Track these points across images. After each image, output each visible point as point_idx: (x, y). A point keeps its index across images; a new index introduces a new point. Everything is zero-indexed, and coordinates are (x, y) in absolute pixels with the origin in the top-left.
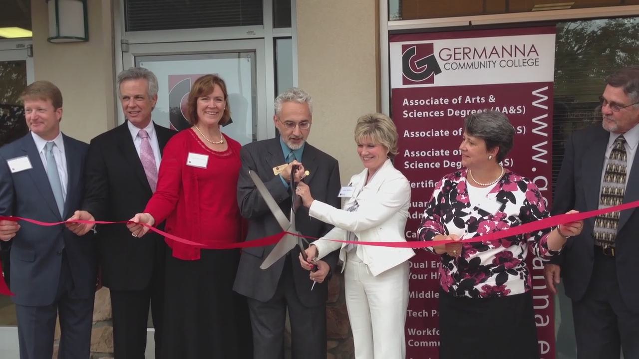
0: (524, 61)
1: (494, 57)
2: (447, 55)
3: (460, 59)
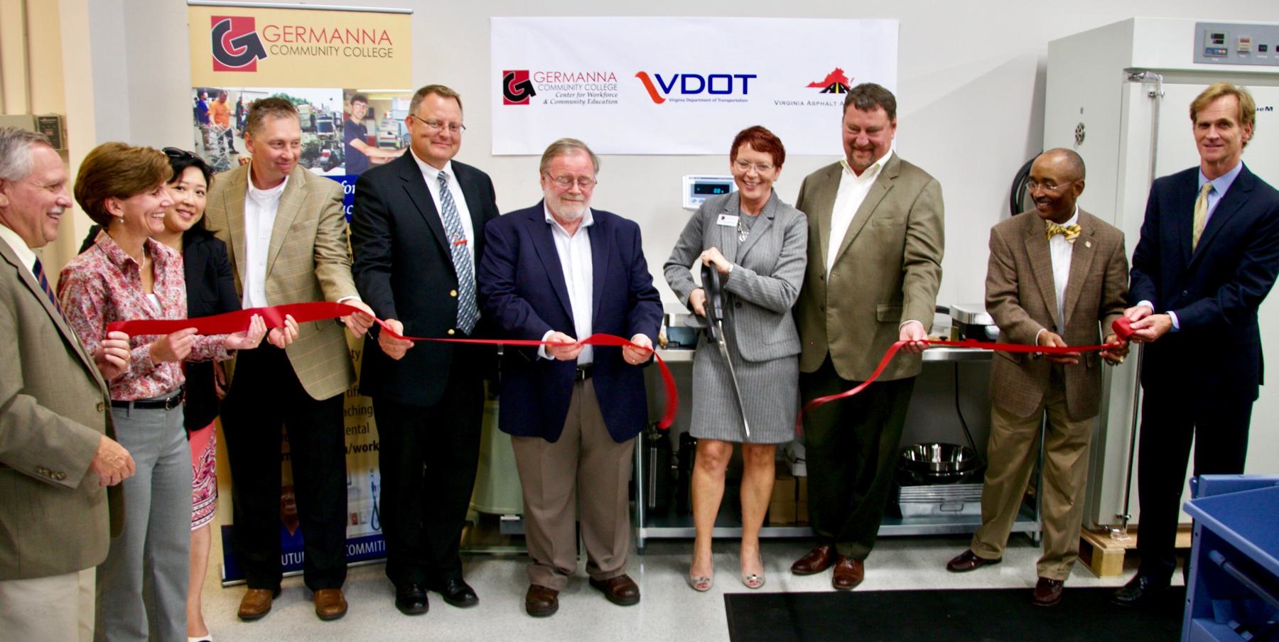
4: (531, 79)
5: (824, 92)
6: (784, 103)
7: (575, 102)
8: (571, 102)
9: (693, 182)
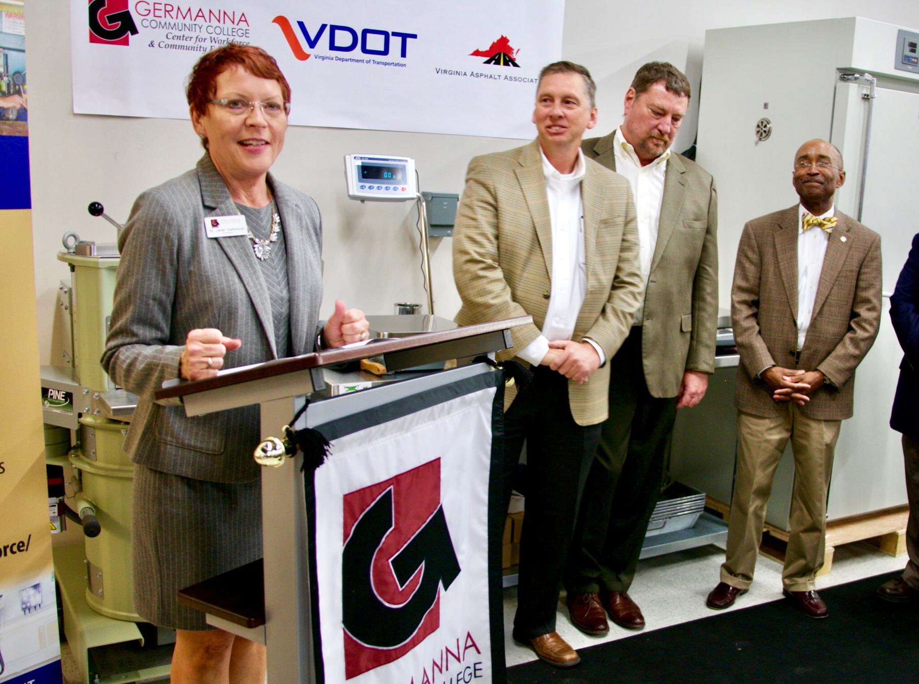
0: (234, 30)
1: (200, 21)
2: (146, 10)
3: (161, 17)
5: (488, 62)
6: (445, 72)
7: (193, 48)
8: (188, 48)
9: (359, 163)
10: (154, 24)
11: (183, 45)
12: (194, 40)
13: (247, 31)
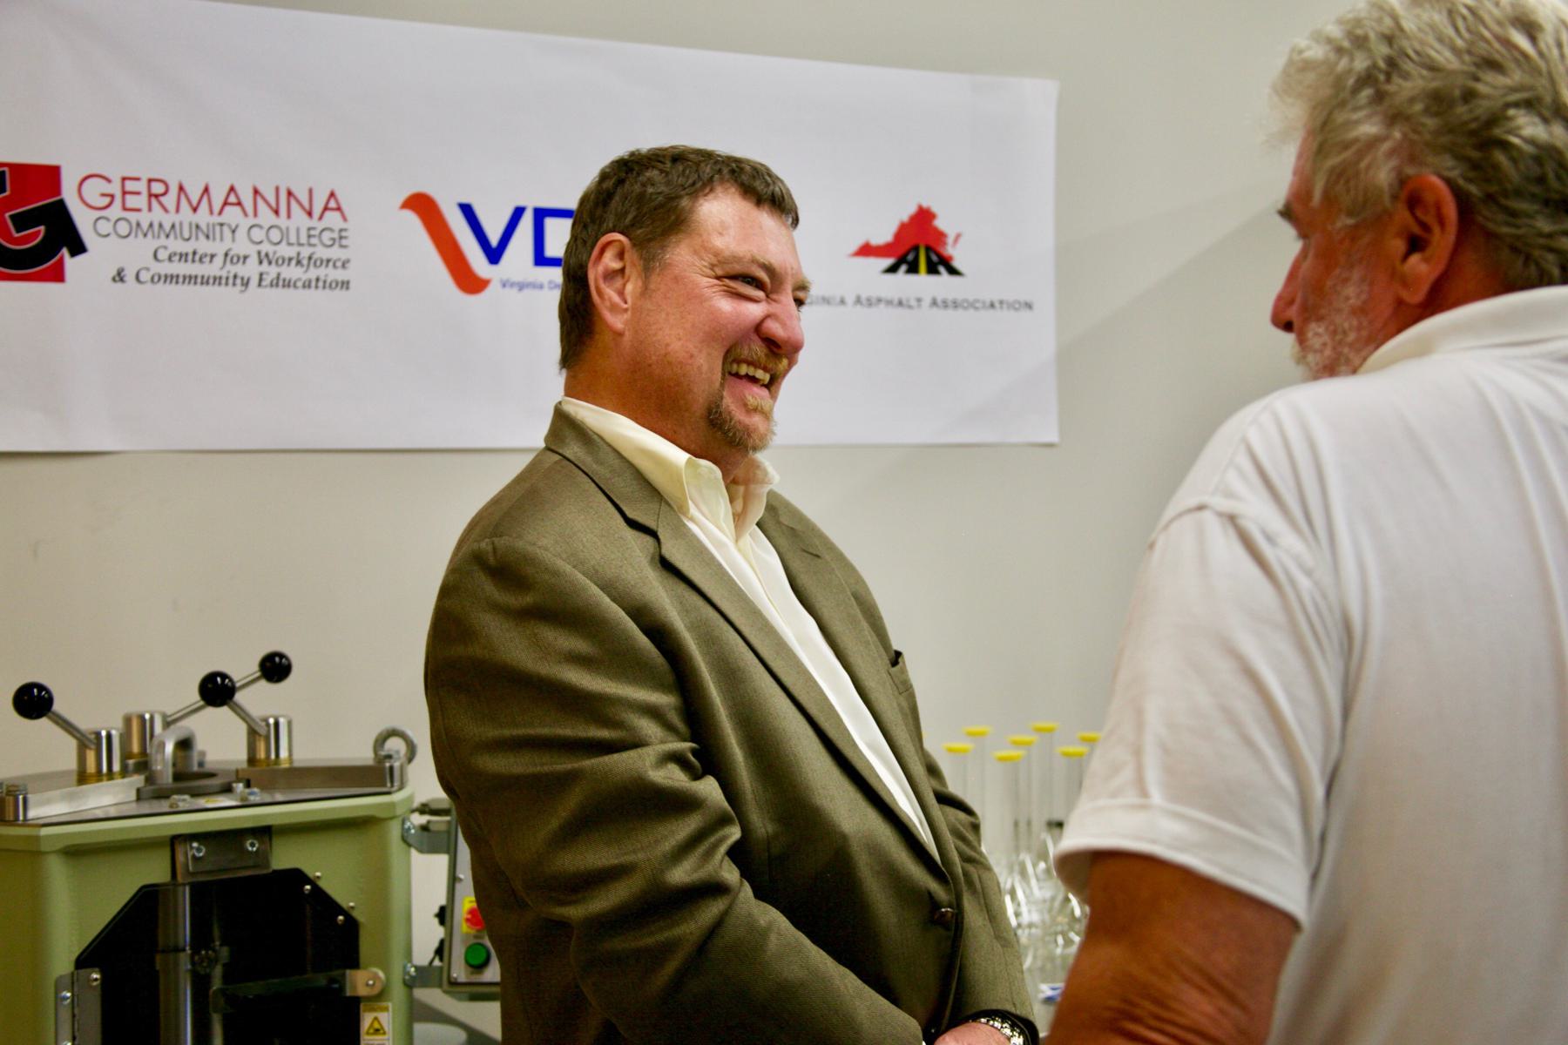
0: (312, 232)
1: (232, 214)
2: (104, 195)
3: (138, 210)
4: (69, 194)
5: (892, 269)
7: (217, 280)
8: (205, 281)
10: (123, 228)
11: (194, 273)
12: (219, 260)
13: (344, 234)
